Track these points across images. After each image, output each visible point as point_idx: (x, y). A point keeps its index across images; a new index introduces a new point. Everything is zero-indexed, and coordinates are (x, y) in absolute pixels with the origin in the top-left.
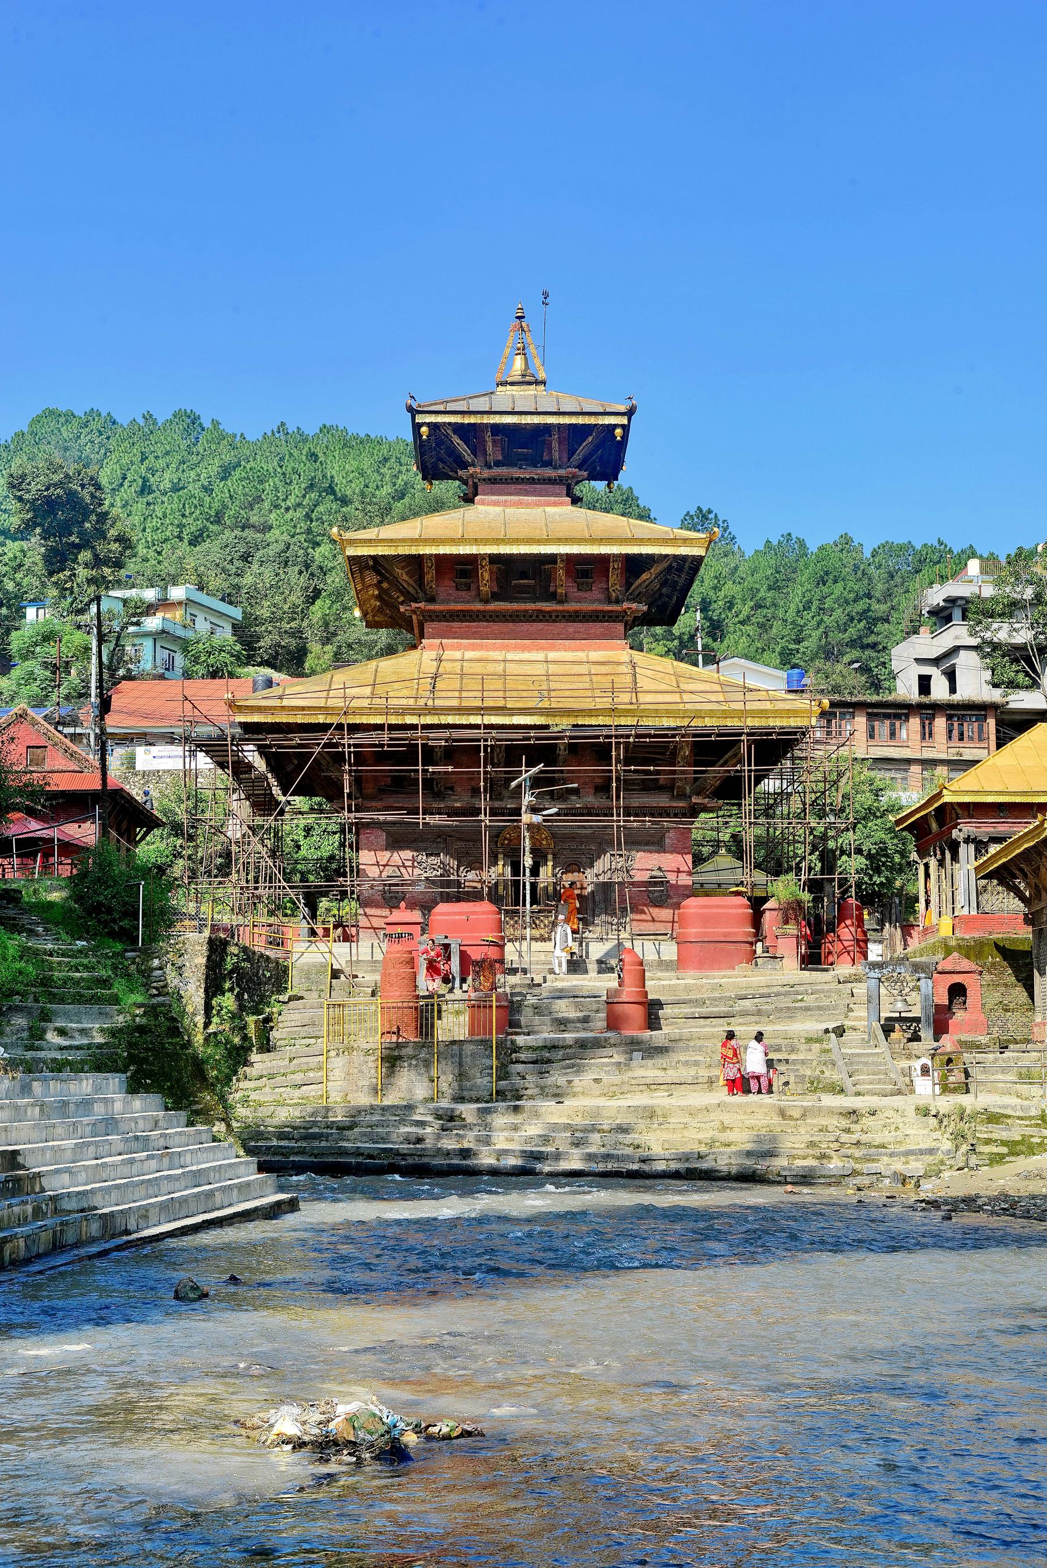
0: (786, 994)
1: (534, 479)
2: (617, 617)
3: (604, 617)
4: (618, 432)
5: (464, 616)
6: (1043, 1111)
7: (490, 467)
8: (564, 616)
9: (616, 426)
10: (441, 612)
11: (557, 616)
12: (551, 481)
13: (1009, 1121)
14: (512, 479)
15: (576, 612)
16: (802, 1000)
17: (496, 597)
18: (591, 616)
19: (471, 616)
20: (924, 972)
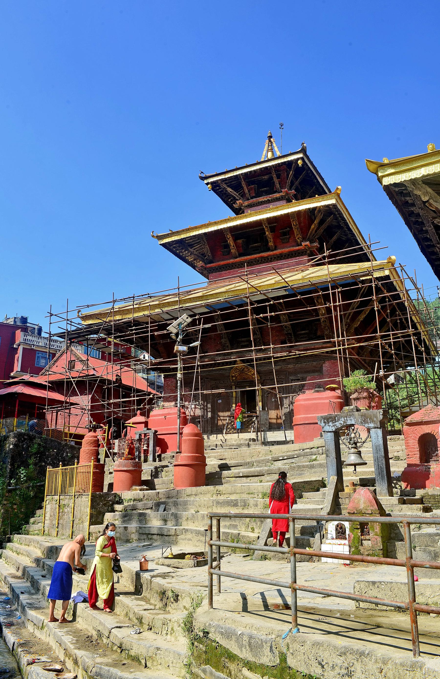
0: (305, 455)
1: (269, 200)
2: (303, 253)
3: (296, 254)
4: (300, 162)
5: (226, 267)
6: (283, 659)
7: (248, 199)
8: (275, 258)
9: (298, 159)
10: (215, 267)
11: (271, 258)
12: (278, 199)
13: (232, 667)
14: (259, 203)
15: (281, 254)
16: (315, 460)
17: (241, 255)
18: (289, 255)
19: (229, 267)
20: (373, 421)
